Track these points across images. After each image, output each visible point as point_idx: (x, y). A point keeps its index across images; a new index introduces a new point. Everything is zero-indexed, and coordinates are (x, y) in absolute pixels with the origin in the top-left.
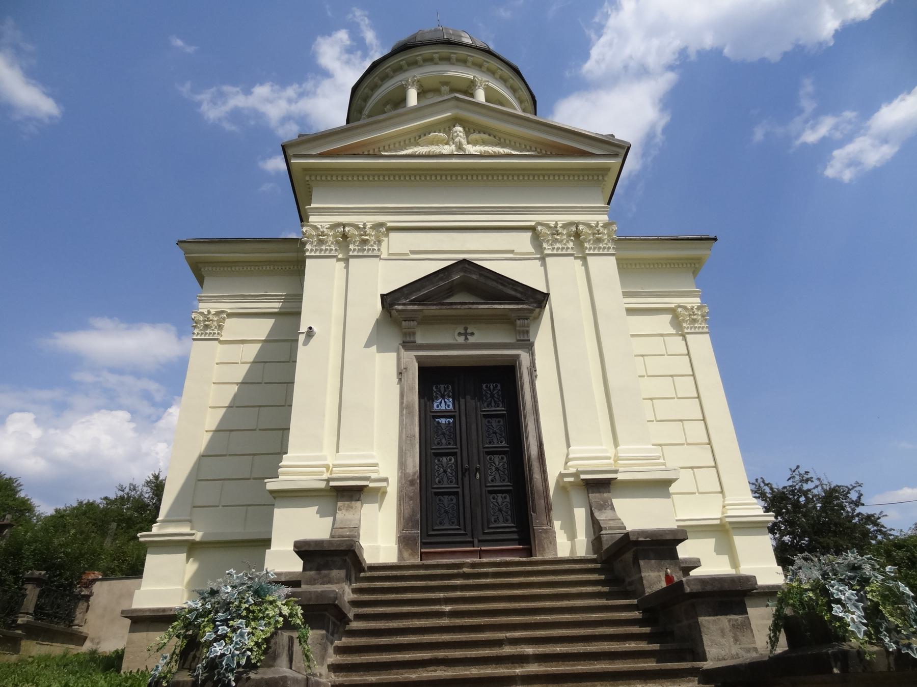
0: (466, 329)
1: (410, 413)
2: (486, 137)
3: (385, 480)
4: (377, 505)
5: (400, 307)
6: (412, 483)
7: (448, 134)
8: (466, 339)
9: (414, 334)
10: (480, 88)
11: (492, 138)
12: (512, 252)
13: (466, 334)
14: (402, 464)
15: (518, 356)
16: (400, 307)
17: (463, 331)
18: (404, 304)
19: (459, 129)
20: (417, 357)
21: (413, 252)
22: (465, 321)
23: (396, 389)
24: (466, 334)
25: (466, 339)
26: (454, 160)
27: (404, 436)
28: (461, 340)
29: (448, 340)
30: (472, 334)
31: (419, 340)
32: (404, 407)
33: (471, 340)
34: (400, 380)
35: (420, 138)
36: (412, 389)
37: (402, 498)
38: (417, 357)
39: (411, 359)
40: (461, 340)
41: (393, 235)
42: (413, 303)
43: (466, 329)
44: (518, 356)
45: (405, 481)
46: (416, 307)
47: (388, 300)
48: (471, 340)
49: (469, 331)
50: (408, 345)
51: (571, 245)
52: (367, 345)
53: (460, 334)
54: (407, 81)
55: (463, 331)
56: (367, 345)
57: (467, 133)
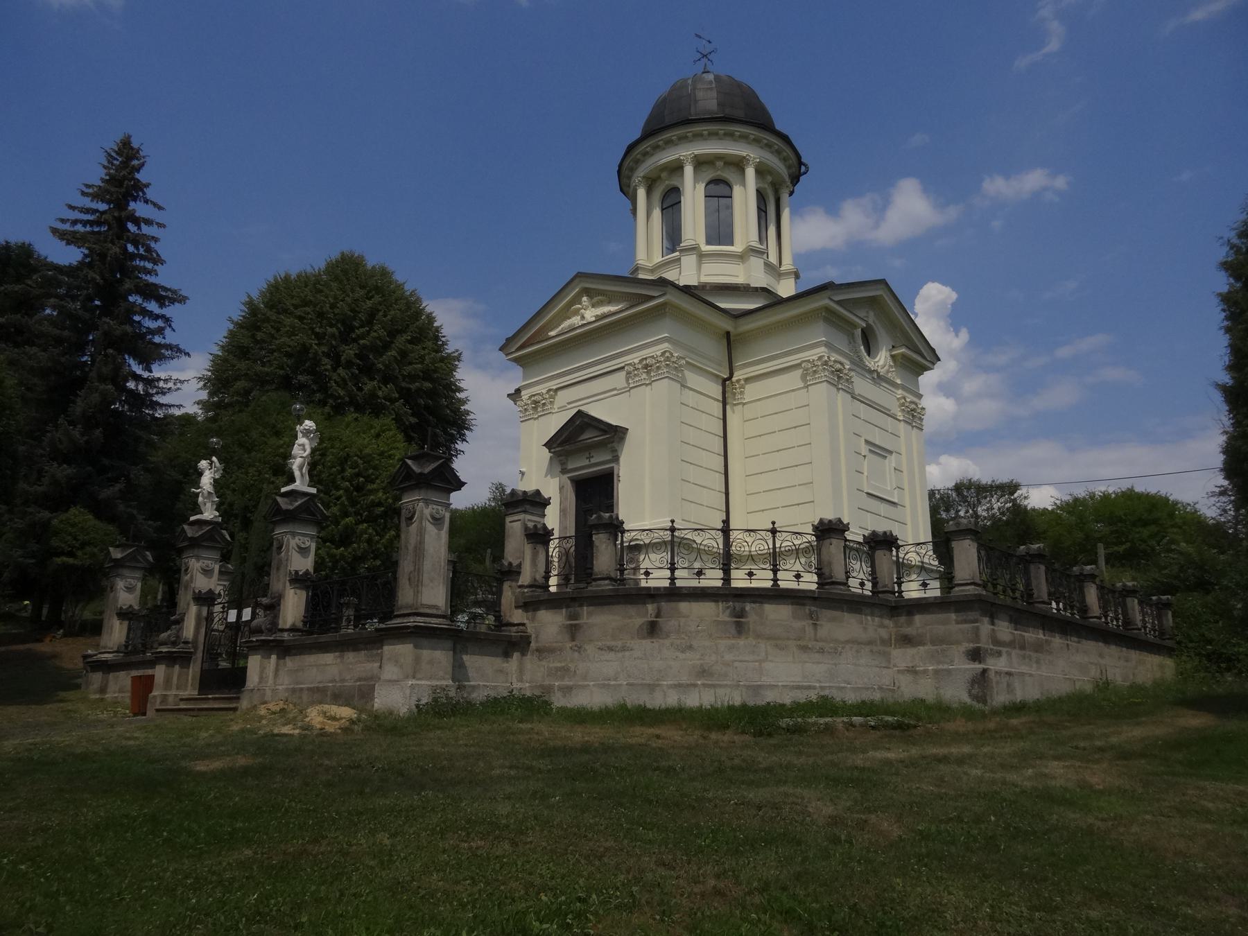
7: (580, 304)
8: (590, 461)
11: (604, 298)
12: (615, 389)
13: (589, 458)
15: (613, 467)
17: (588, 456)
18: (554, 448)
20: (568, 477)
21: (569, 403)
24: (589, 458)
25: (590, 461)
26: (578, 331)
28: (587, 462)
30: (593, 457)
31: (570, 466)
33: (593, 461)
38: (568, 477)
41: (559, 393)
43: (590, 454)
44: (613, 467)
48: (593, 461)
50: (564, 471)
51: (644, 376)
52: (546, 476)
53: (587, 458)
55: (588, 456)
56: (546, 476)
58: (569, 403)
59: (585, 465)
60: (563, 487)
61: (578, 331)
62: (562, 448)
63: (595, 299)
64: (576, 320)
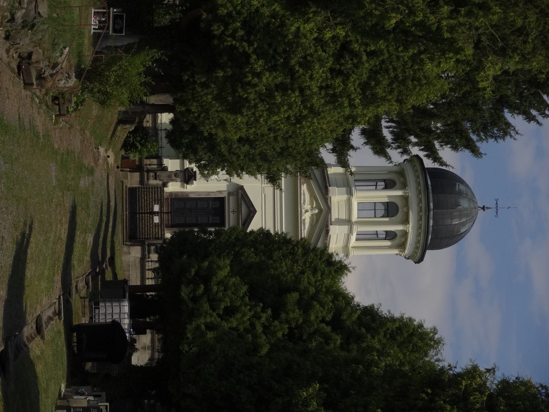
0: (235, 212)
1: (207, 195)
2: (315, 221)
3: (186, 188)
4: (180, 186)
5: (240, 191)
6: (187, 195)
7: (316, 207)
8: (232, 212)
9: (233, 196)
10: (404, 228)
11: (314, 223)
13: (233, 212)
14: (192, 193)
16: (240, 191)
17: (234, 211)
18: (241, 192)
19: (317, 211)
21: (265, 195)
22: (238, 211)
23: (215, 191)
24: (233, 212)
25: (232, 212)
27: (200, 193)
28: (231, 210)
29: (231, 207)
30: (233, 214)
31: (231, 198)
32: (209, 193)
33: (231, 214)
34: (218, 192)
35: (314, 197)
36: (215, 195)
37: (182, 192)
39: (225, 195)
40: (231, 210)
42: (242, 195)
43: (235, 212)
45: (187, 193)
46: (240, 196)
47: (242, 188)
48: (231, 214)
49: (234, 213)
50: (230, 194)
53: (233, 210)
54: (408, 190)
55: (234, 211)
57: (317, 214)
58: (265, 195)
59: (230, 205)
60: (221, 193)
61: (299, 209)
62: (240, 198)
63: (315, 217)
64: (307, 206)
